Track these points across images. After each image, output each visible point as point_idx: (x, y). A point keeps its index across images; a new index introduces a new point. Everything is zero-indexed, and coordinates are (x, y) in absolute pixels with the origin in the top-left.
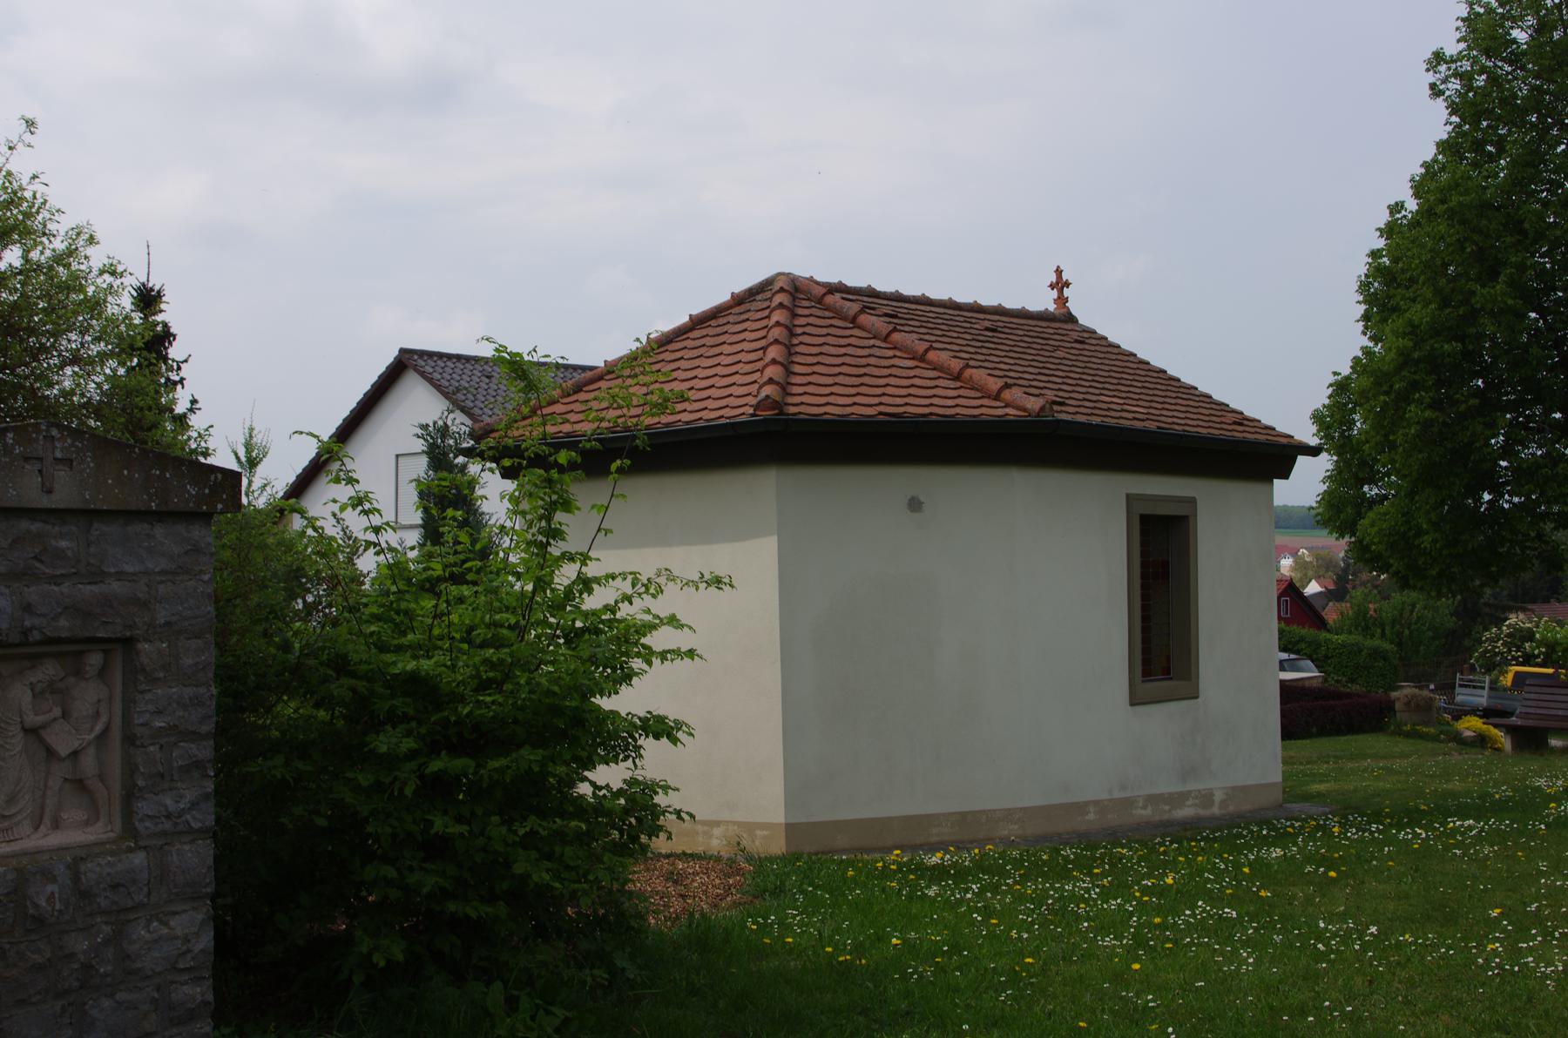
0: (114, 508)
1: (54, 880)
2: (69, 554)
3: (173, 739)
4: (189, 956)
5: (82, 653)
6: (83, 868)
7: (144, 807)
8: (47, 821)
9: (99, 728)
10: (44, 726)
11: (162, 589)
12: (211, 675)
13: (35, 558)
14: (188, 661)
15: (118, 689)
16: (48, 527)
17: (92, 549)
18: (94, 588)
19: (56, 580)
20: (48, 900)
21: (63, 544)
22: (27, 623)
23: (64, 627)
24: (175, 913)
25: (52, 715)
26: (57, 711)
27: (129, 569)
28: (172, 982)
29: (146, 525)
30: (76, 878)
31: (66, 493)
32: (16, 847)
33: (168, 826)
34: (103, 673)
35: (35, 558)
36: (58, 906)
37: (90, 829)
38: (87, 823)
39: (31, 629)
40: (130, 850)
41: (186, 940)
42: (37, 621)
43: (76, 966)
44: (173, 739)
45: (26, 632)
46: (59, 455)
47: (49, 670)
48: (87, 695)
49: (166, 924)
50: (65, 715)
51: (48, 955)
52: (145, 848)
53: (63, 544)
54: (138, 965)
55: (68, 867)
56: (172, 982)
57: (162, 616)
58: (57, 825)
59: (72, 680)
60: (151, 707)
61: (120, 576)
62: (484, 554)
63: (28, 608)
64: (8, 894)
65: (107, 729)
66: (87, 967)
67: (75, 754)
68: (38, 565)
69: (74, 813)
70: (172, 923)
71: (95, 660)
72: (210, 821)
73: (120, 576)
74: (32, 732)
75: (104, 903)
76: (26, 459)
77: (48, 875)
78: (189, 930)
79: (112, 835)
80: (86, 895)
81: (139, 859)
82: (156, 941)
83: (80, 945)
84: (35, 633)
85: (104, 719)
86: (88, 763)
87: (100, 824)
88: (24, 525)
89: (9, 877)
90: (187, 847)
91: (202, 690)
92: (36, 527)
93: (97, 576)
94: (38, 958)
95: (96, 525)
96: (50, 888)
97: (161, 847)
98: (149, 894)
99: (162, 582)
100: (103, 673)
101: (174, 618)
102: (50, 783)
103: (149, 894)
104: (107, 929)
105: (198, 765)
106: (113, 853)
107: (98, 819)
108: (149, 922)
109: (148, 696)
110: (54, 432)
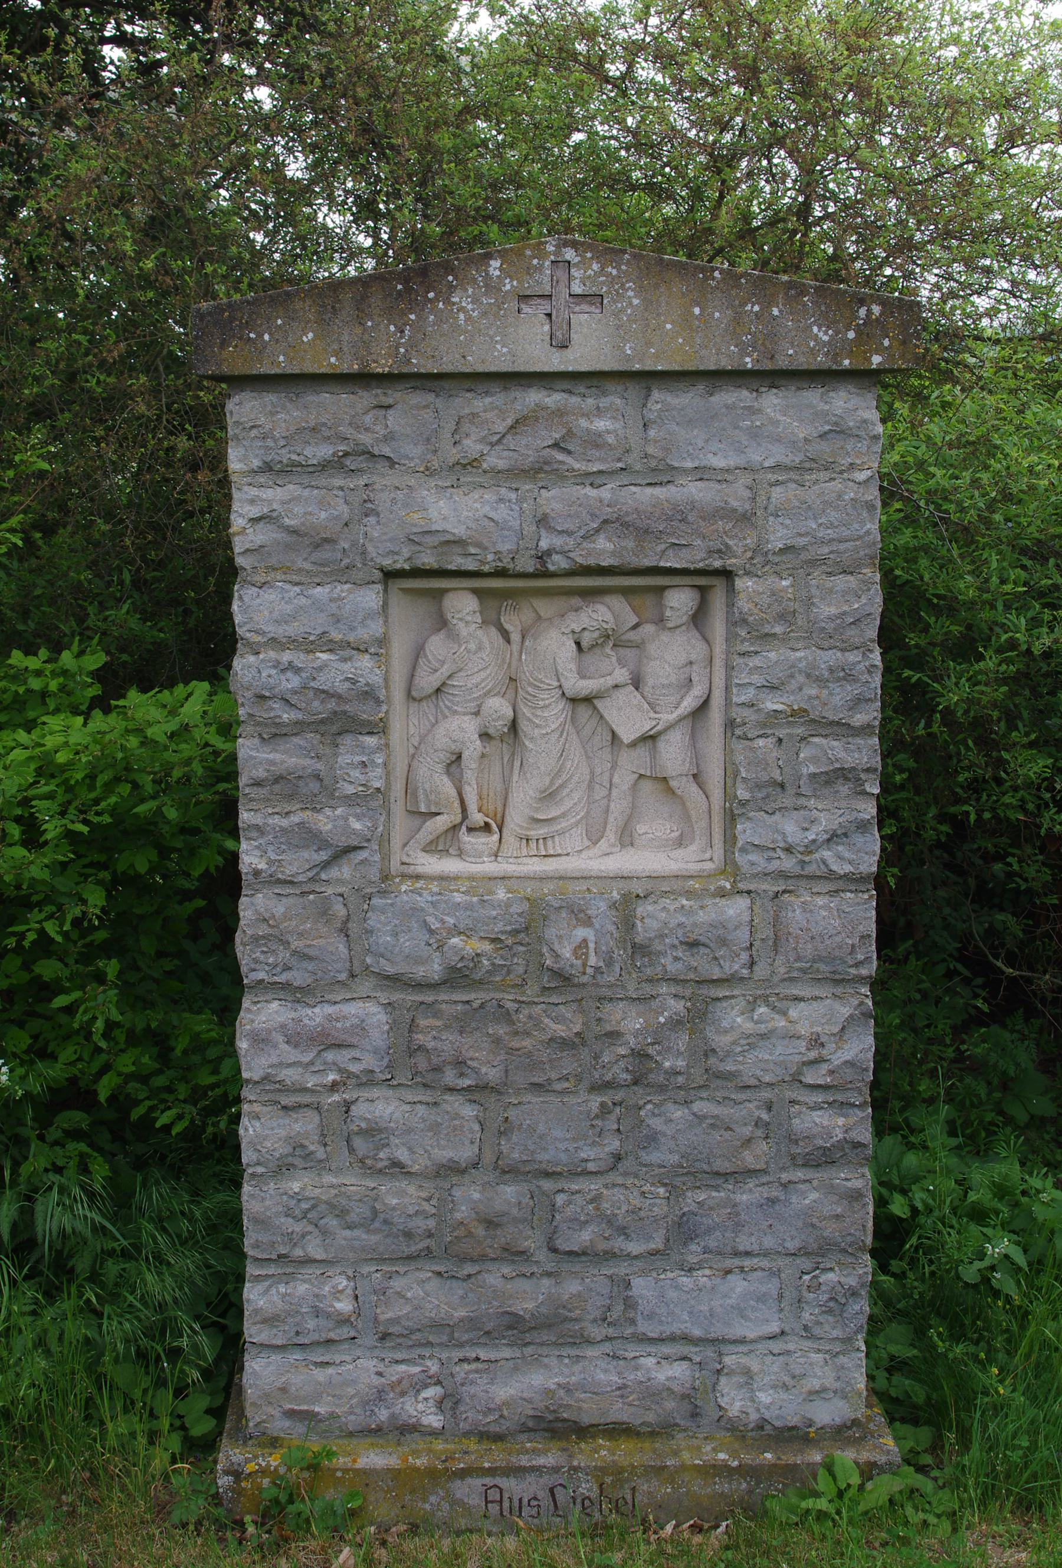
0: (677, 368)
1: (588, 922)
2: (611, 439)
3: (800, 731)
4: (824, 1068)
5: (663, 589)
6: (640, 911)
7: (745, 832)
8: (611, 835)
9: (689, 703)
10: (599, 696)
11: (777, 493)
12: (873, 633)
13: (556, 445)
14: (826, 610)
15: (719, 647)
16: (574, 400)
17: (652, 433)
18: (657, 491)
19: (593, 479)
20: (575, 952)
21: (601, 424)
22: (544, 544)
23: (604, 549)
24: (798, 999)
25: (610, 681)
26: (621, 675)
27: (718, 462)
28: (792, 1102)
29: (745, 393)
30: (627, 924)
31: (592, 345)
32: (550, 866)
33: (788, 864)
34: (698, 618)
35: (556, 445)
36: (593, 960)
37: (679, 853)
38: (680, 842)
39: (549, 553)
40: (722, 894)
41: (816, 1042)
42: (558, 541)
43: (622, 1051)
44: (800, 731)
45: (542, 557)
46: (577, 289)
47: (599, 615)
48: (671, 652)
49: (784, 1013)
50: (637, 683)
51: (577, 1028)
52: (749, 892)
53: (601, 424)
54: (730, 1067)
55: (613, 906)
56: (792, 1102)
57: (778, 536)
58: (626, 838)
59: (649, 628)
60: (757, 679)
61: (701, 473)
62: (207, 361)
63: (543, 521)
64: (515, 932)
65: (704, 705)
66: (640, 1055)
67: (650, 739)
68: (561, 457)
69: (656, 825)
70: (793, 1013)
71: (680, 601)
72: (870, 864)
73: (701, 473)
74: (582, 702)
75: (672, 968)
76: (524, 298)
77: (581, 916)
78: (830, 1030)
79: (709, 866)
80: (639, 949)
81: (736, 908)
82: (763, 1036)
83: (631, 1022)
84: (556, 557)
85: (698, 691)
86: (673, 754)
87: (693, 848)
88: (534, 397)
89: (516, 909)
90: (820, 901)
91: (852, 657)
92: (553, 399)
93: (661, 474)
94: (560, 1030)
95: (656, 395)
96: (581, 933)
97: (777, 895)
98: (752, 964)
99: (777, 483)
100: (698, 618)
101: (802, 541)
102: (616, 780)
103: (752, 964)
104: (678, 1006)
105: (842, 774)
106: (689, 894)
107: (693, 840)
108: (752, 1006)
109: (755, 661)
110: (569, 254)
